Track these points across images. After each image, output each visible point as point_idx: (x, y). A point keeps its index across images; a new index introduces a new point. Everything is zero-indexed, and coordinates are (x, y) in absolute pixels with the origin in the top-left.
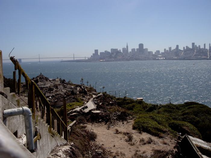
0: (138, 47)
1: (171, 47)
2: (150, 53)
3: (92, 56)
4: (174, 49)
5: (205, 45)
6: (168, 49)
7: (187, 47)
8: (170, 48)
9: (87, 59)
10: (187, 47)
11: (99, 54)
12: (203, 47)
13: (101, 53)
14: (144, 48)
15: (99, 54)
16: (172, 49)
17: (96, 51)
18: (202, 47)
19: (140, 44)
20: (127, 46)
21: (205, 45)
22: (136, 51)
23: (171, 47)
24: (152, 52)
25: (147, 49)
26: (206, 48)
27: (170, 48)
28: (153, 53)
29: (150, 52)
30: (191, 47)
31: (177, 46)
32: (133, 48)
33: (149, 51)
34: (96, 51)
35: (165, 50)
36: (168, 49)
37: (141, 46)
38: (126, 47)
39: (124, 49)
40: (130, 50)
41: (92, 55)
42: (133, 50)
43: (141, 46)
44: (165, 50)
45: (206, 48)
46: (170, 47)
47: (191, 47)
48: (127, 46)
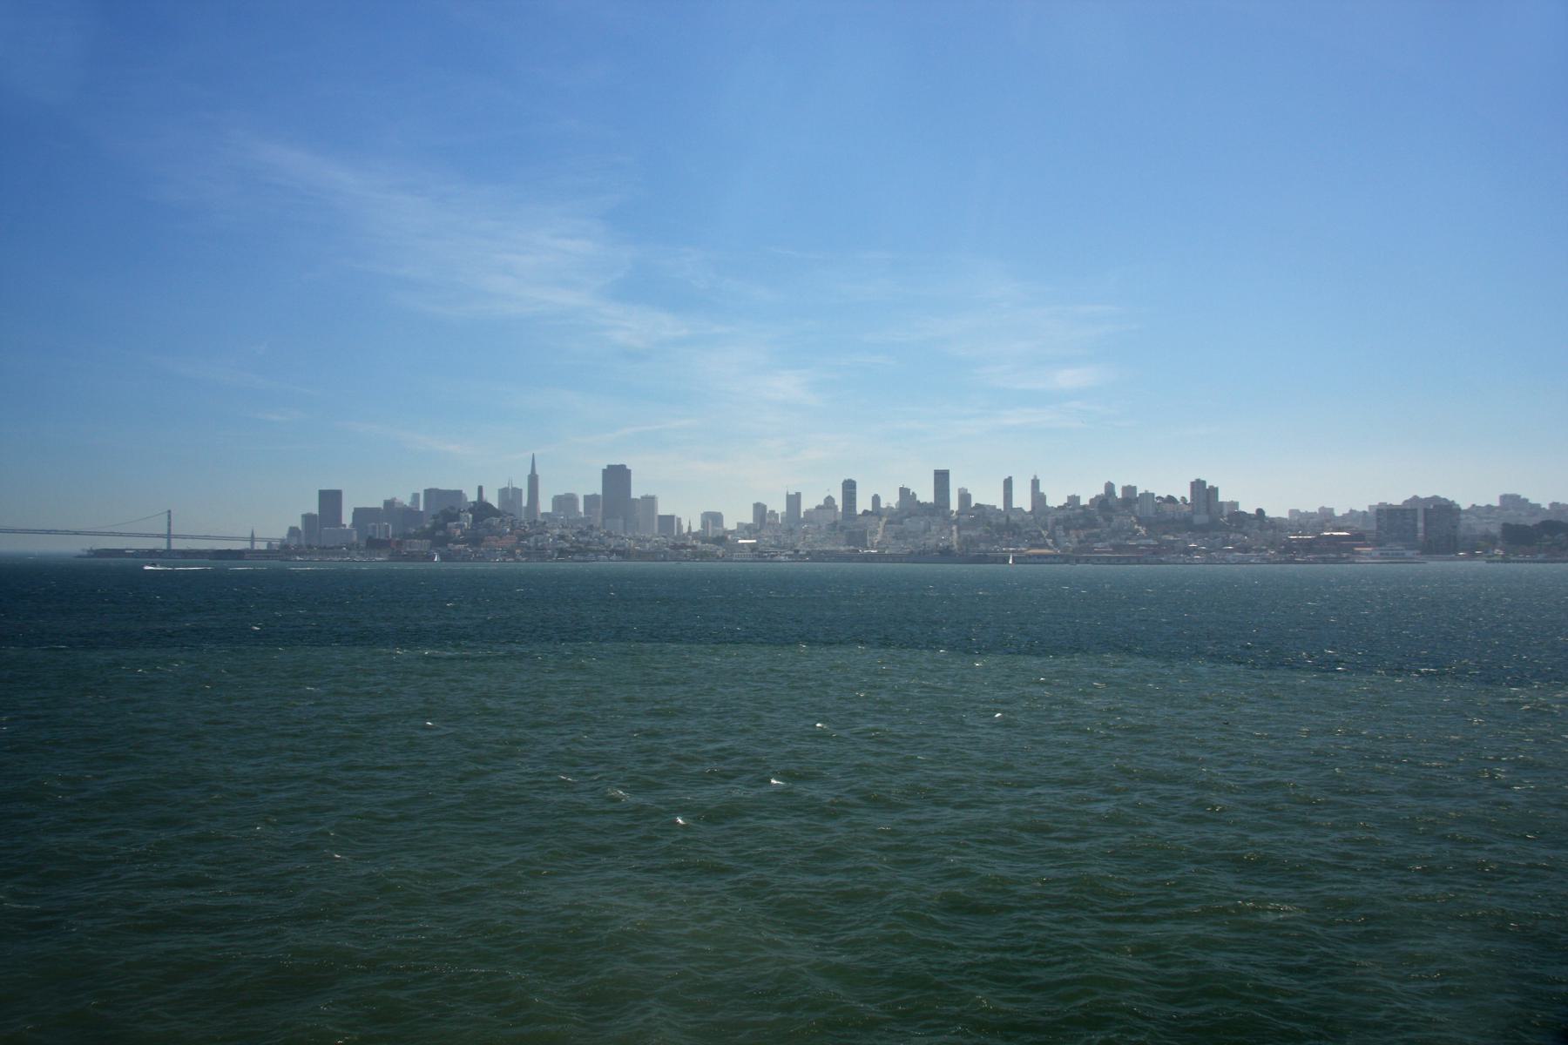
0: (597, 489)
1: (798, 495)
2: (669, 521)
3: (293, 531)
4: (819, 508)
5: (1008, 484)
6: (779, 507)
7: (904, 492)
8: (794, 500)
9: (262, 546)
10: (904, 492)
11: (347, 519)
12: (1000, 506)
13: (358, 513)
14: (636, 493)
15: (347, 519)
16: (808, 503)
17: (330, 500)
18: (988, 495)
19: (609, 466)
20: (533, 480)
21: (1008, 484)
22: (581, 509)
23: (798, 495)
24: (679, 519)
25: (650, 501)
26: (1015, 505)
27: (794, 500)
28: (680, 527)
29: (672, 517)
30: (926, 495)
31: (849, 488)
32: (561, 493)
33: (663, 509)
34: (330, 500)
35: (759, 509)
36: (779, 507)
37: (617, 477)
38: (523, 485)
39: (508, 494)
40: (545, 506)
41: (298, 523)
42: (564, 502)
43: (617, 477)
44: (759, 509)
45: (1015, 505)
46: (792, 492)
47: (926, 495)
48: (533, 480)
